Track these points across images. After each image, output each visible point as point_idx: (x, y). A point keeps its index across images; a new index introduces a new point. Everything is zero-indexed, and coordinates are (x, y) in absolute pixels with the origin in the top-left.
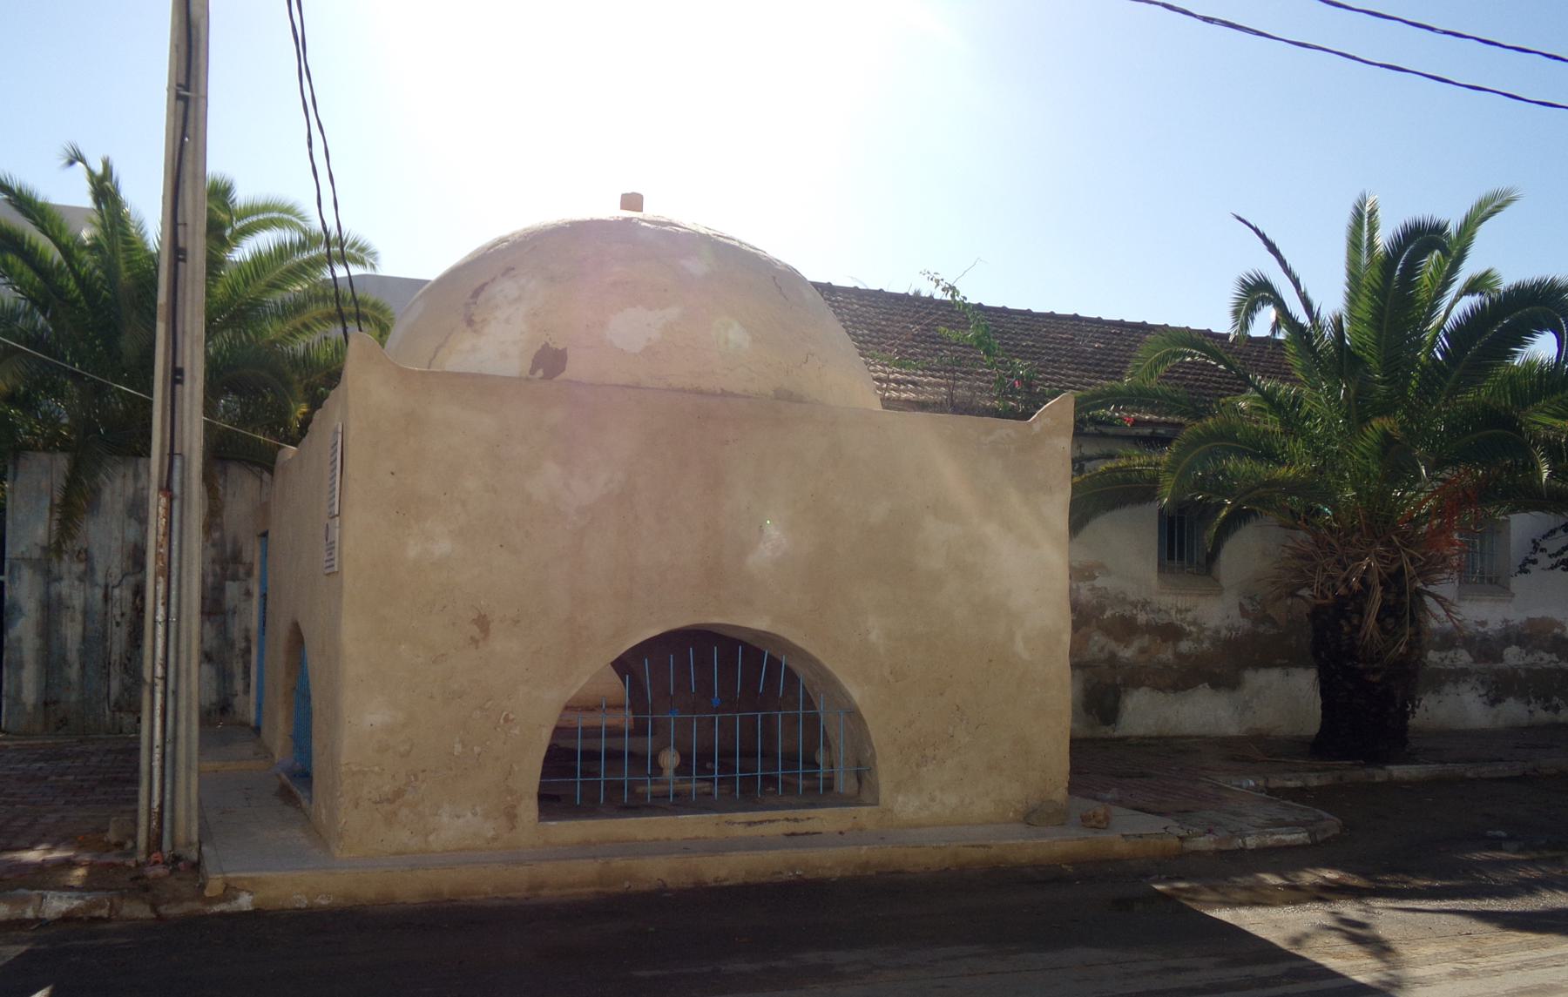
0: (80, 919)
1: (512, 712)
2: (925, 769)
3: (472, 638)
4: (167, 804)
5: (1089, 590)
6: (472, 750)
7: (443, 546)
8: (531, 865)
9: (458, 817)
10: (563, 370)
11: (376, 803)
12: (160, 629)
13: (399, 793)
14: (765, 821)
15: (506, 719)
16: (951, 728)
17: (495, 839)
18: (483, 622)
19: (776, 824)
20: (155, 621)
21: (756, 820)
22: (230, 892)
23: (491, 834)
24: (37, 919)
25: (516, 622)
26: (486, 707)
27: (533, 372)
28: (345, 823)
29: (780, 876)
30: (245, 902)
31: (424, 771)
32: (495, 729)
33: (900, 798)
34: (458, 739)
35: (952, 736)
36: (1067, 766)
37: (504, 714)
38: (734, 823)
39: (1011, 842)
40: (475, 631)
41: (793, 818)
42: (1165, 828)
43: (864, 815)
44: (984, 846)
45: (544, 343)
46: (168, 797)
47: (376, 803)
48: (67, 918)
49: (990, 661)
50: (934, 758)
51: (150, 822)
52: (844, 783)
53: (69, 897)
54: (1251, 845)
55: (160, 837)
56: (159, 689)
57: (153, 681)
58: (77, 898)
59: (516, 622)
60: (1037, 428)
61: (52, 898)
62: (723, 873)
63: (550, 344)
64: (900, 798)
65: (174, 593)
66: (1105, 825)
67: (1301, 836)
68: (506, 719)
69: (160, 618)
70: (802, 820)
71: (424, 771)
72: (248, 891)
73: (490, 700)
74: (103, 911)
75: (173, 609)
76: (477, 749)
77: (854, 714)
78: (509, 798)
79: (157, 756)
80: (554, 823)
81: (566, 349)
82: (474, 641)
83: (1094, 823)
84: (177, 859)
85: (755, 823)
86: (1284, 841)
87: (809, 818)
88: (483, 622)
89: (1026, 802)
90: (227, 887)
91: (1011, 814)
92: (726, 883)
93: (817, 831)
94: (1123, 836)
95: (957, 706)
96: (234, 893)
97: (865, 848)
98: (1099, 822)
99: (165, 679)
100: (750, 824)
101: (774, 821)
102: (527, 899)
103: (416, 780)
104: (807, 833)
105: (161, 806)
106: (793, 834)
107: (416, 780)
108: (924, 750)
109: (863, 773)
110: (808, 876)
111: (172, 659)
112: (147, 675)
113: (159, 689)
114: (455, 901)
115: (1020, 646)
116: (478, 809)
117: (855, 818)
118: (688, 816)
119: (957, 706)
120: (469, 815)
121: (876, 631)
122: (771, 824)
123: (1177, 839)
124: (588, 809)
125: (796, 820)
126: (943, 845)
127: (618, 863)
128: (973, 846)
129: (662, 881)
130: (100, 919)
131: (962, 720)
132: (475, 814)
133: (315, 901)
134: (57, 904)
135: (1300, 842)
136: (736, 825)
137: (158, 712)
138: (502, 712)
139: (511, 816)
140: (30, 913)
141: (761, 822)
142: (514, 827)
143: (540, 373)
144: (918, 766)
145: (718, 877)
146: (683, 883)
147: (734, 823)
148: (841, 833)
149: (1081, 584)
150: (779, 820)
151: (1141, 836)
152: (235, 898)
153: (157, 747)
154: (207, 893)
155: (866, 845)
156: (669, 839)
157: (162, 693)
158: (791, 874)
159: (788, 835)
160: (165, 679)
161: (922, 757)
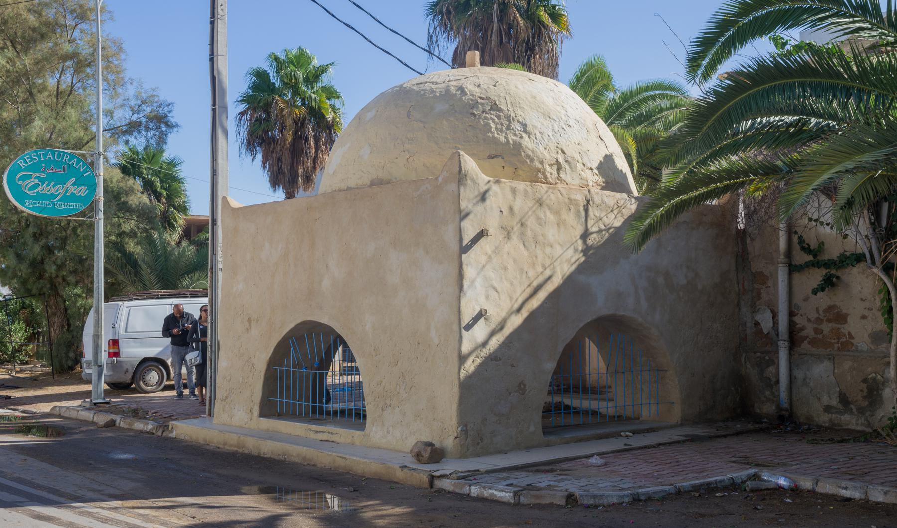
13: (227, 397)
16: (398, 387)
33: (374, 429)
40: (247, 324)
44: (345, 458)
49: (419, 343)
50: (390, 406)
54: (474, 493)
62: (266, 451)
67: (507, 494)
76: (246, 380)
86: (496, 496)
88: (249, 320)
92: (265, 456)
97: (305, 448)
100: (317, 432)
120: (242, 410)
125: (332, 433)
127: (242, 438)
128: (341, 457)
131: (403, 383)
135: (505, 500)
144: (382, 409)
159: (321, 441)
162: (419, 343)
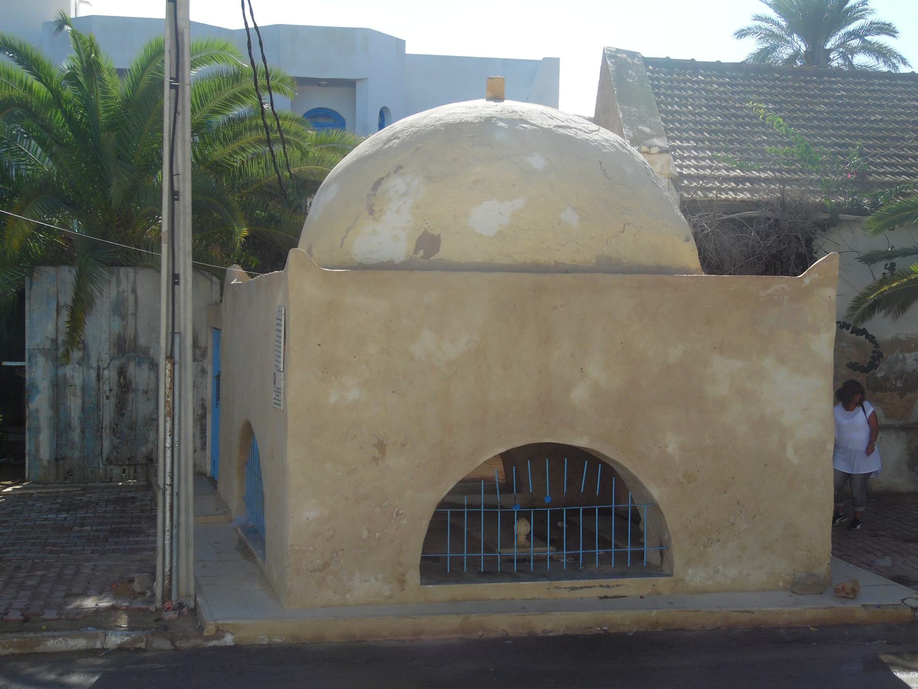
0: (128, 650)
1: (401, 509)
2: (711, 549)
3: (374, 457)
4: (174, 570)
5: (914, 360)
6: (375, 535)
7: (354, 394)
8: (415, 618)
9: (366, 582)
10: (438, 251)
11: (311, 572)
12: (169, 453)
13: (326, 565)
14: (585, 587)
15: (398, 514)
17: (391, 597)
18: (381, 446)
19: (592, 589)
20: (165, 447)
21: (577, 587)
22: (219, 633)
23: (389, 593)
24: (103, 649)
25: (403, 445)
26: (384, 505)
27: (416, 252)
28: (291, 585)
29: (591, 630)
30: (229, 640)
31: (342, 550)
32: (390, 520)
33: (690, 571)
34: (364, 528)
35: (734, 524)
36: (828, 546)
37: (396, 511)
38: (560, 588)
39: (770, 609)
40: (376, 452)
41: (605, 585)
42: (903, 600)
43: (661, 582)
44: (748, 612)
45: (424, 230)
46: (175, 564)
47: (311, 572)
48: (120, 649)
49: (766, 465)
51: (164, 581)
52: (651, 555)
53: (122, 635)
55: (170, 591)
56: (168, 492)
57: (165, 487)
58: (127, 635)
59: (403, 445)
60: (807, 281)
61: (111, 635)
62: (549, 627)
63: (428, 229)
64: (690, 571)
65: (176, 427)
66: (851, 596)
68: (398, 514)
69: (168, 445)
70: (613, 587)
71: (342, 550)
72: (230, 633)
73: (386, 500)
74: (142, 644)
75: (176, 438)
76: (378, 535)
77: (655, 506)
78: (400, 569)
79: (168, 537)
80: (431, 586)
81: (440, 235)
82: (375, 459)
83: (843, 595)
84: (181, 606)
85: (576, 588)
87: (618, 586)
88: (381, 446)
89: (794, 574)
90: (218, 630)
91: (781, 584)
92: (551, 634)
93: (624, 595)
94: (864, 606)
95: (738, 501)
96: (222, 633)
97: (655, 611)
98: (847, 593)
99: (172, 485)
100: (573, 589)
101: (591, 587)
102: (412, 641)
103: (337, 556)
104: (616, 597)
105: (171, 570)
106: (606, 597)
107: (337, 556)
108: (710, 534)
109: (663, 550)
110: (612, 631)
111: (176, 472)
112: (161, 483)
113: (168, 492)
114: (364, 641)
115: (790, 453)
116: (379, 576)
117: (654, 585)
118: (527, 583)
119: (738, 501)
121: (672, 444)
122: (589, 589)
123: (910, 610)
124: (455, 575)
125: (608, 587)
126: (716, 610)
127: (474, 618)
128: (740, 612)
129: (505, 631)
130: (140, 649)
132: (377, 579)
133: (274, 640)
134: (114, 640)
136: (562, 589)
137: (168, 508)
138: (395, 508)
139: (402, 582)
140: (99, 645)
141: (581, 588)
142: (404, 589)
143: (421, 253)
144: (704, 546)
145: (545, 630)
146: (520, 633)
147: (560, 588)
148: (642, 597)
149: (907, 355)
150: (595, 587)
151: (879, 607)
152: (223, 637)
153: (168, 531)
154: (205, 634)
155: (655, 609)
156: (512, 599)
157: (170, 495)
158: (599, 629)
159: (601, 598)
160: (172, 485)
161: (709, 540)
162: (766, 465)
